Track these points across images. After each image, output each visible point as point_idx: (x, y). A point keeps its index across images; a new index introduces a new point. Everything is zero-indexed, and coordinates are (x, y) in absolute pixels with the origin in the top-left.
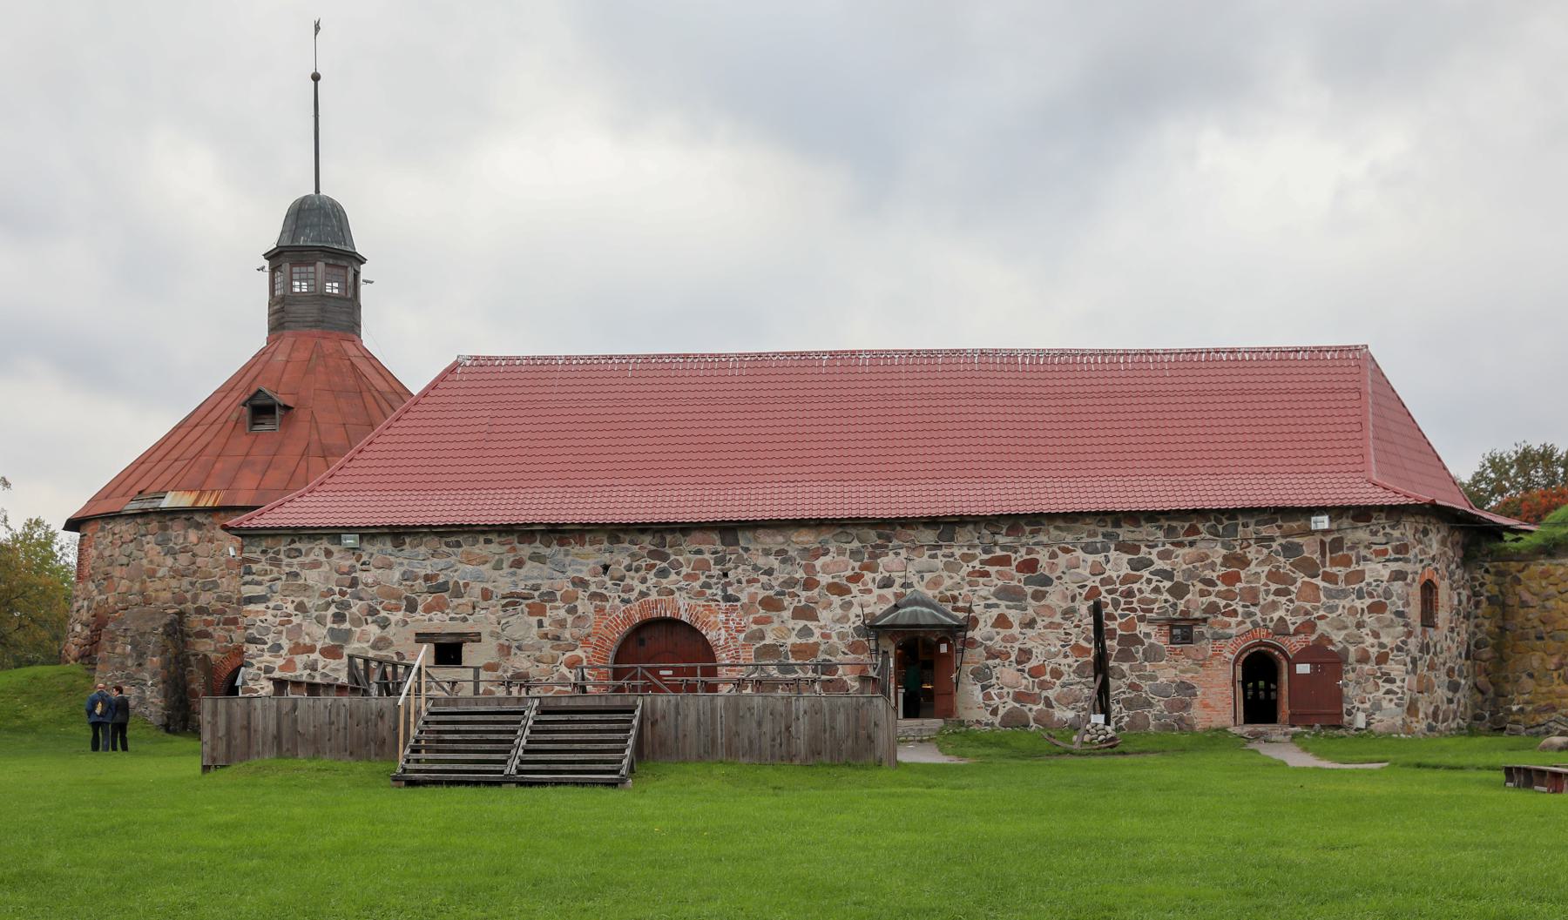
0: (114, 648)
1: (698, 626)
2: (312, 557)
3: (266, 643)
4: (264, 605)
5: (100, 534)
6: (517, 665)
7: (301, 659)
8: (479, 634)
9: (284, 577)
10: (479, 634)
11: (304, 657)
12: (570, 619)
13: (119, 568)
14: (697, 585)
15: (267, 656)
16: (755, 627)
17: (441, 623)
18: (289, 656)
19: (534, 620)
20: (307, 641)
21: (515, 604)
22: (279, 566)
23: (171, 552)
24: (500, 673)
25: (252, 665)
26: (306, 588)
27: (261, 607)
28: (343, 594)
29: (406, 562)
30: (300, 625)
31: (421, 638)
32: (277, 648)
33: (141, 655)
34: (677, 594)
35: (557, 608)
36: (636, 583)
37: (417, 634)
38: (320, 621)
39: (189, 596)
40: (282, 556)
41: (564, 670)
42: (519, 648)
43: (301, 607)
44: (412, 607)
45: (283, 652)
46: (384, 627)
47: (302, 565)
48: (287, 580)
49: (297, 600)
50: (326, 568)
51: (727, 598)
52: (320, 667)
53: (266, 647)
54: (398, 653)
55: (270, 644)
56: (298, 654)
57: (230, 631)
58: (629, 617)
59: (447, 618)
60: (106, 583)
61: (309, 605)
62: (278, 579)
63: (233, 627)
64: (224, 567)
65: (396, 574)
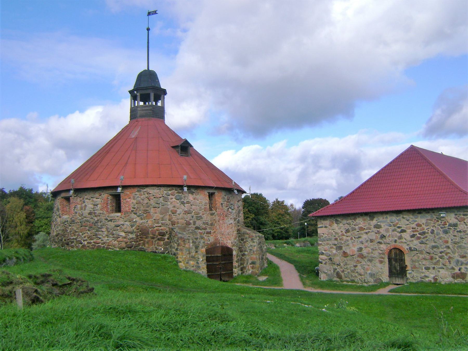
0: (185, 244)
5: (137, 193)
13: (152, 209)
23: (183, 203)
33: (197, 247)
39: (191, 221)
57: (209, 236)
60: (145, 215)
63: (209, 235)
64: (203, 210)
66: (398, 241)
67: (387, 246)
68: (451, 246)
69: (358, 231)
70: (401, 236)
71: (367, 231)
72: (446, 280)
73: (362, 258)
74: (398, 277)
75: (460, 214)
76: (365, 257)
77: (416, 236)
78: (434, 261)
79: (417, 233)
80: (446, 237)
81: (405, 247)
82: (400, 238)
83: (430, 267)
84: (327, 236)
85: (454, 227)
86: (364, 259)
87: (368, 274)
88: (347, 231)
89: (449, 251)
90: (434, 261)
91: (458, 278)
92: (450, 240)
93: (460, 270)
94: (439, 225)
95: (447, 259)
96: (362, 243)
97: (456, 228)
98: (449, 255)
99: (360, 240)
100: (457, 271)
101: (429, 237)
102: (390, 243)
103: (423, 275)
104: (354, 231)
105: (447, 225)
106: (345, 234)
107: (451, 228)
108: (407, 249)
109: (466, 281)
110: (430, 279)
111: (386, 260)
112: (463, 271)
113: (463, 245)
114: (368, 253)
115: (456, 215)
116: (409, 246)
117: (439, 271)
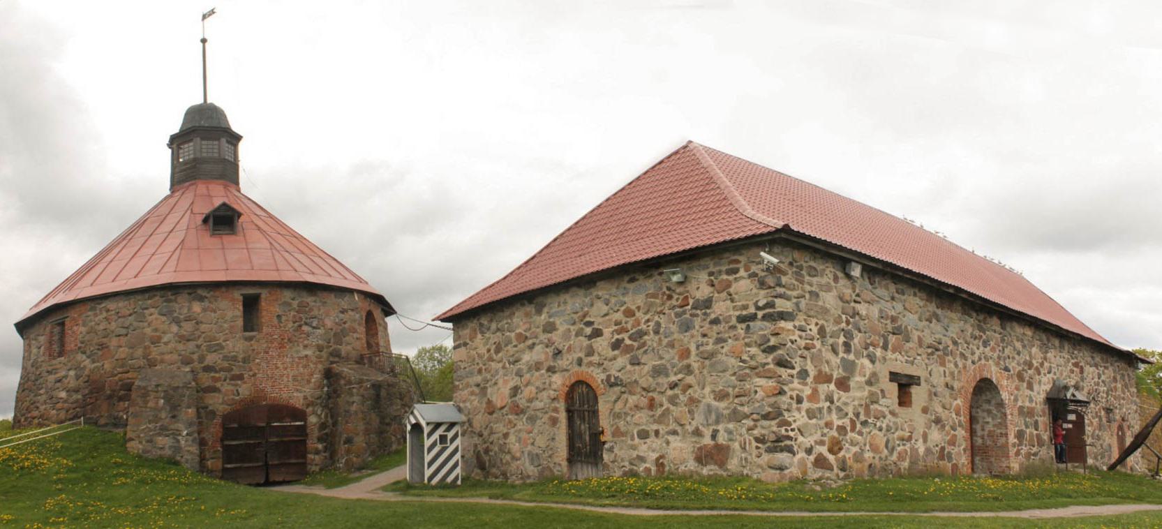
1: (999, 387)
2: (824, 280)
3: (793, 368)
4: (792, 324)
6: (936, 410)
7: (823, 389)
8: (919, 378)
9: (807, 296)
10: (919, 378)
11: (826, 385)
12: (956, 373)
14: (995, 355)
15: (796, 384)
16: (1016, 392)
17: (899, 363)
18: (813, 386)
19: (942, 369)
20: (826, 369)
21: (932, 354)
22: (802, 282)
24: (928, 416)
25: (785, 392)
26: (825, 311)
27: (789, 325)
28: (848, 323)
29: (877, 299)
30: (820, 350)
31: (894, 376)
32: (803, 374)
34: (990, 360)
35: (950, 361)
36: (975, 348)
37: (891, 373)
38: (835, 351)
40: (804, 272)
41: (954, 416)
42: (935, 395)
43: (822, 331)
44: (885, 348)
45: (810, 380)
46: (873, 362)
47: (820, 286)
48: (810, 300)
49: (821, 322)
50: (834, 293)
51: (1006, 369)
52: (835, 399)
53: (794, 372)
54: (882, 391)
55: (798, 369)
56: (820, 383)
58: (975, 375)
59: (903, 360)
61: (828, 330)
62: (802, 297)
65: (875, 311)
66: (586, 361)
67: (564, 377)
68: (695, 366)
69: (515, 346)
70: (591, 347)
71: (530, 342)
72: (683, 468)
73: (517, 414)
74: (588, 463)
75: (720, 272)
76: (523, 412)
77: (622, 345)
78: (659, 411)
79: (625, 336)
80: (686, 340)
81: (597, 376)
82: (590, 352)
83: (648, 432)
84: (466, 366)
85: (703, 311)
86: (522, 416)
87: (526, 455)
88: (498, 350)
89: (690, 379)
90: (659, 411)
91: (710, 464)
92: (693, 348)
93: (714, 437)
94: (673, 308)
95: (686, 405)
96: (519, 374)
97: (708, 311)
98: (690, 391)
99: (518, 366)
100: (707, 441)
101: (649, 343)
102: (568, 368)
103: (635, 454)
104: (509, 347)
105: (689, 307)
106: (494, 355)
107: (699, 312)
108: (602, 380)
109: (727, 470)
110: (648, 465)
111: (563, 416)
112: (722, 439)
113: (724, 358)
114: (530, 400)
115: (711, 274)
116: (608, 373)
117: (668, 443)
